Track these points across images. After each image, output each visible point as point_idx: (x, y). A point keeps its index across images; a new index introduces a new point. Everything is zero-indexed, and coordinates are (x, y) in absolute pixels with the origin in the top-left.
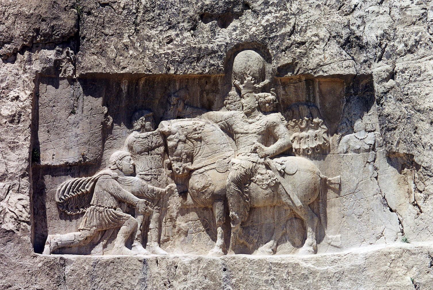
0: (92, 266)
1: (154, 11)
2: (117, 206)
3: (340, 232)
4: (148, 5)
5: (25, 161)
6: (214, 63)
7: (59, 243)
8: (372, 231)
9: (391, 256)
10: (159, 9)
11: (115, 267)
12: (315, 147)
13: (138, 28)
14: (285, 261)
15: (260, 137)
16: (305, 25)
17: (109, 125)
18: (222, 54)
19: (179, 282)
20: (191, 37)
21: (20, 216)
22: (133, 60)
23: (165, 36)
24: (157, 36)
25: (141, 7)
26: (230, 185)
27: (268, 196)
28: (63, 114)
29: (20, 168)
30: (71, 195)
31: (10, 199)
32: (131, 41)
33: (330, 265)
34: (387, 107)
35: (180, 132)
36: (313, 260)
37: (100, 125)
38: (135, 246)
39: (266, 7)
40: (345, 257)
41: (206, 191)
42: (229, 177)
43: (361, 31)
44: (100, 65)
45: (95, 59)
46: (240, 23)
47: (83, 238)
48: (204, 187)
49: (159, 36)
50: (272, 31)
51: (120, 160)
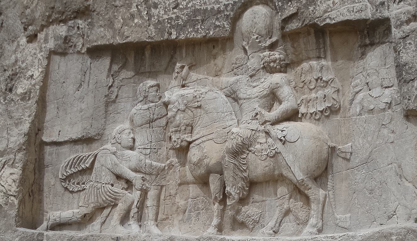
2: (114, 182)
5: (23, 136)
6: (219, 24)
9: (392, 238)
12: (324, 109)
17: (113, 98)
18: (228, 13)
21: (9, 190)
28: (71, 88)
29: (18, 143)
30: (72, 171)
31: (4, 173)
32: (139, 10)
37: (104, 99)
38: (130, 224)
45: (101, 31)
48: (200, 160)
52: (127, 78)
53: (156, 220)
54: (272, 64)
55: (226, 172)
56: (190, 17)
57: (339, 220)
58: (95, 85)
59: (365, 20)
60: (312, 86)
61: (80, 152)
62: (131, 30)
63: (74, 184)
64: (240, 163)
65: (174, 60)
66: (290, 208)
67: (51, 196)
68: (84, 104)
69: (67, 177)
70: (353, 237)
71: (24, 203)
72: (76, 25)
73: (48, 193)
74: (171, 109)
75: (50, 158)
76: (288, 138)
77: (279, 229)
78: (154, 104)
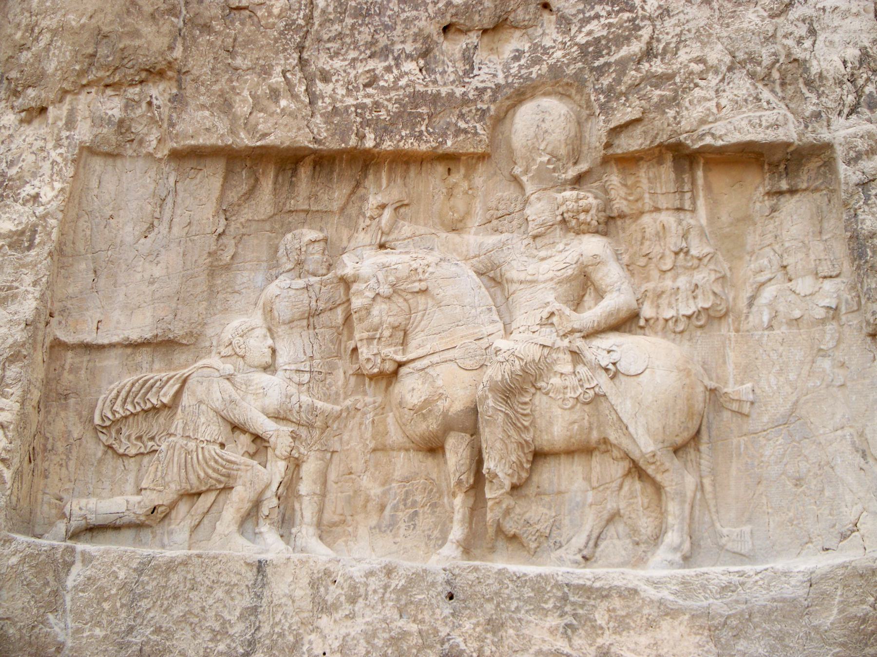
0: (135, 570)
1: (342, 21)
3: (749, 521)
4: (331, 9)
5: (23, 325)
7: (89, 517)
8: (830, 517)
10: (351, 16)
11: (189, 576)
12: (694, 313)
13: (305, 55)
14: (603, 582)
15: (561, 290)
16: (674, 40)
18: (485, 107)
19: (335, 621)
20: (417, 71)
22: (286, 120)
23: (360, 71)
24: (345, 71)
25: (316, 14)
26: (487, 397)
27: (576, 426)
28: (128, 232)
29: (10, 341)
32: (288, 82)
33: (718, 596)
34: (870, 217)
35: (381, 278)
36: (674, 582)
39: (588, 7)
40: (757, 578)
41: (430, 411)
42: (485, 379)
43: (806, 50)
44: (213, 130)
45: (205, 117)
46: (529, 44)
47: (145, 510)
48: (427, 402)
49: (349, 70)
50: (598, 55)
51: (242, 336)
52: (256, 218)
53: (319, 524)
54: (582, 217)
55: (487, 430)
56: (404, 106)
57: (726, 538)
58: (186, 229)
59: (788, 145)
60: (665, 264)
61: (144, 370)
62: (272, 121)
63: (129, 438)
64: (517, 412)
65: (361, 191)
66: (619, 510)
67: (72, 464)
68: (159, 267)
69: (113, 422)
70: (785, 574)
71: (22, 476)
72: (145, 97)
73: (65, 457)
74: (360, 293)
75: (71, 377)
76: (621, 367)
77: (594, 552)
78: (318, 279)
